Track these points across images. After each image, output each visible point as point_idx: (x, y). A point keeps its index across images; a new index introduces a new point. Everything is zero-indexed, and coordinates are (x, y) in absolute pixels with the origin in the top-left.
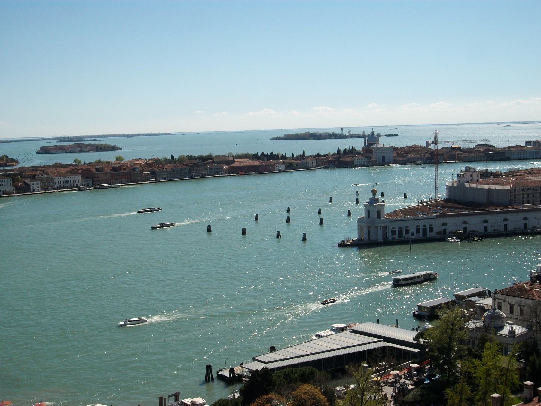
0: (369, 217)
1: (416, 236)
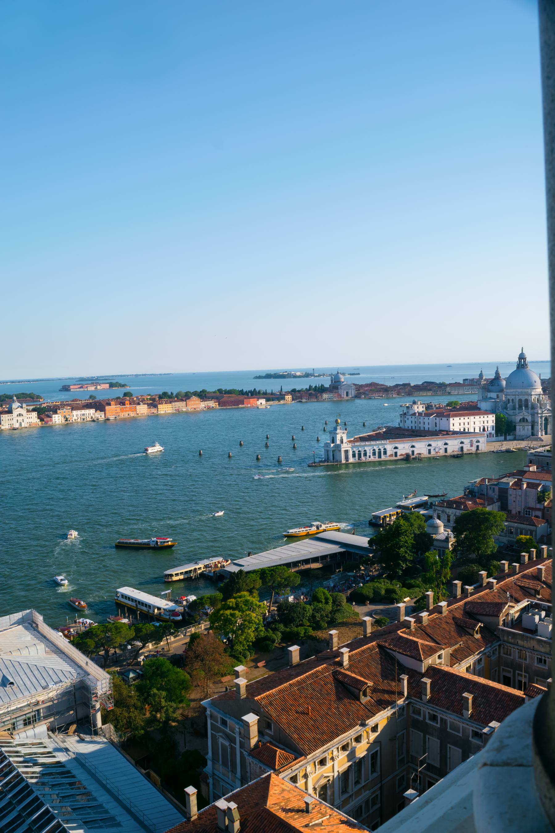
1: (372, 458)
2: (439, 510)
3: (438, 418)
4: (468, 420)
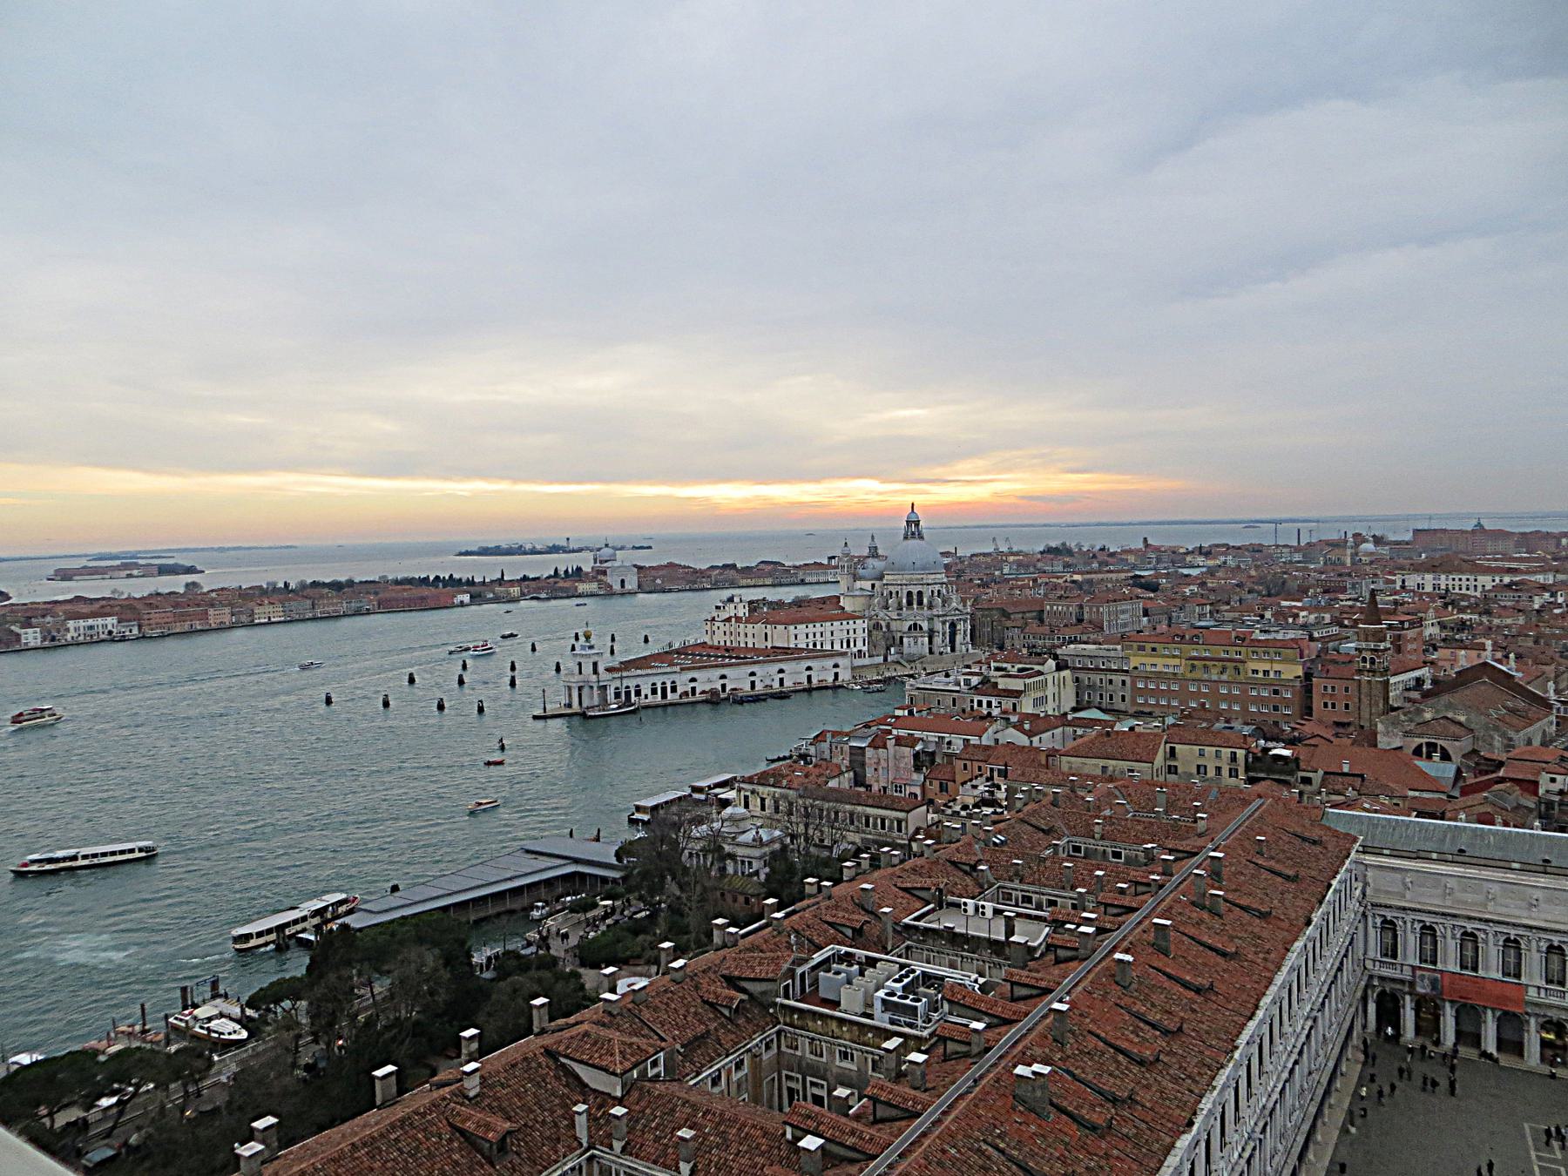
2: (746, 790)
3: (769, 626)
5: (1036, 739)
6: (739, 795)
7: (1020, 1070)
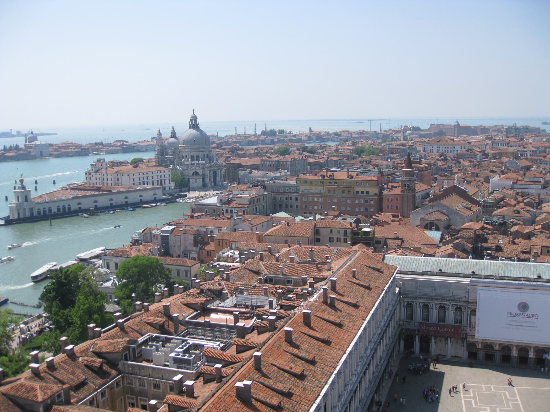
0: (18, 201)
4: (147, 175)
5: (254, 228)
6: (104, 262)
7: (239, 384)
